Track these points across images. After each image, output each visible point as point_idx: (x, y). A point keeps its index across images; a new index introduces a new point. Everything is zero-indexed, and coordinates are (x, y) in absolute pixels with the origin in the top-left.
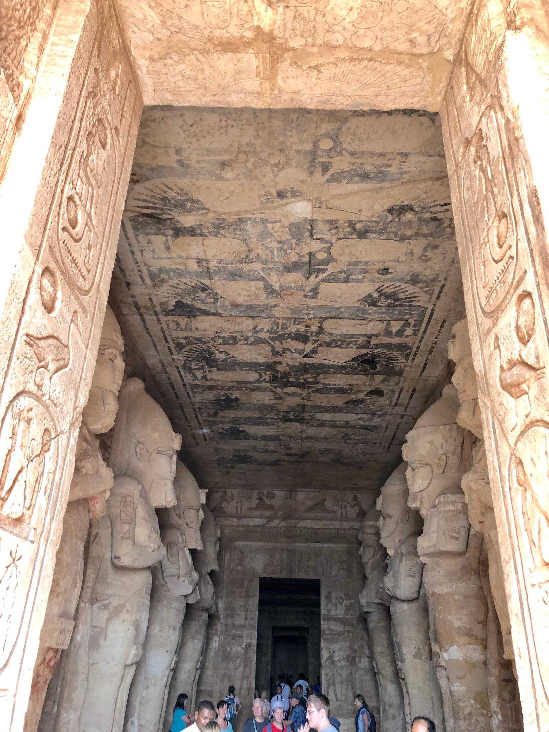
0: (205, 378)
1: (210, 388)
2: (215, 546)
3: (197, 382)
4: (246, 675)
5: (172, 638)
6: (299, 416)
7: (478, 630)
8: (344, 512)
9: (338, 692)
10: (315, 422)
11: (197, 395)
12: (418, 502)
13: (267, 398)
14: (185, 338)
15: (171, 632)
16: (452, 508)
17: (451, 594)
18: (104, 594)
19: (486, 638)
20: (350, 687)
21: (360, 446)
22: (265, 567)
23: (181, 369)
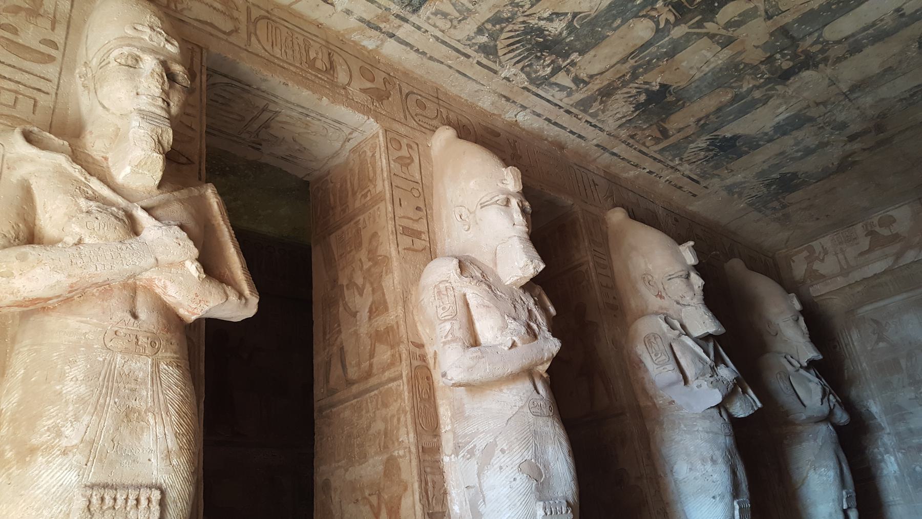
0: (577, 80)
1: (606, 93)
3: (578, 96)
5: (715, 476)
6: (795, 56)
11: (601, 116)
13: (709, 55)
14: (480, 31)
18: (465, 436)
23: (534, 89)
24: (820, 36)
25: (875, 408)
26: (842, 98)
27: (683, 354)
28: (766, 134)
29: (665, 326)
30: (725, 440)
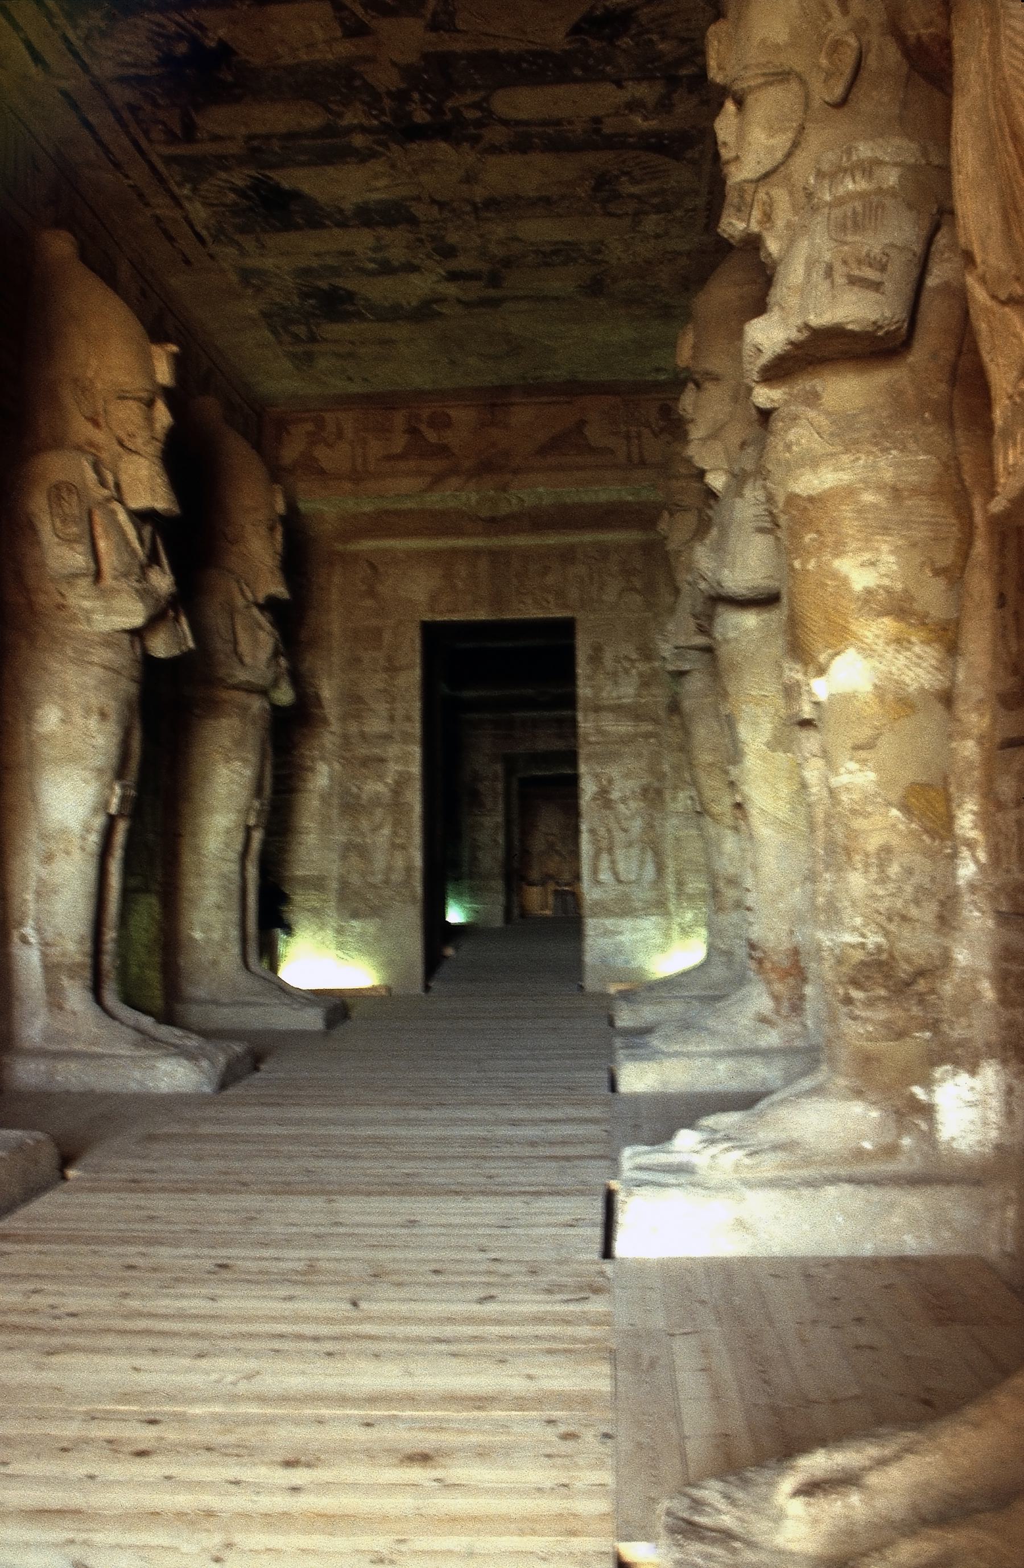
2: (272, 537)
4: (398, 841)
7: (932, 596)
8: (635, 450)
9: (621, 867)
10: (496, 135)
12: (756, 214)
13: (320, 35)
15: (93, 723)
16: (863, 185)
17: (849, 492)
19: (958, 623)
20: (649, 856)
21: (651, 223)
22: (434, 599)
24: (486, 99)
25: (328, 691)
26: (468, 208)
27: (106, 531)
28: (341, 211)
29: (91, 475)
30: (129, 688)
